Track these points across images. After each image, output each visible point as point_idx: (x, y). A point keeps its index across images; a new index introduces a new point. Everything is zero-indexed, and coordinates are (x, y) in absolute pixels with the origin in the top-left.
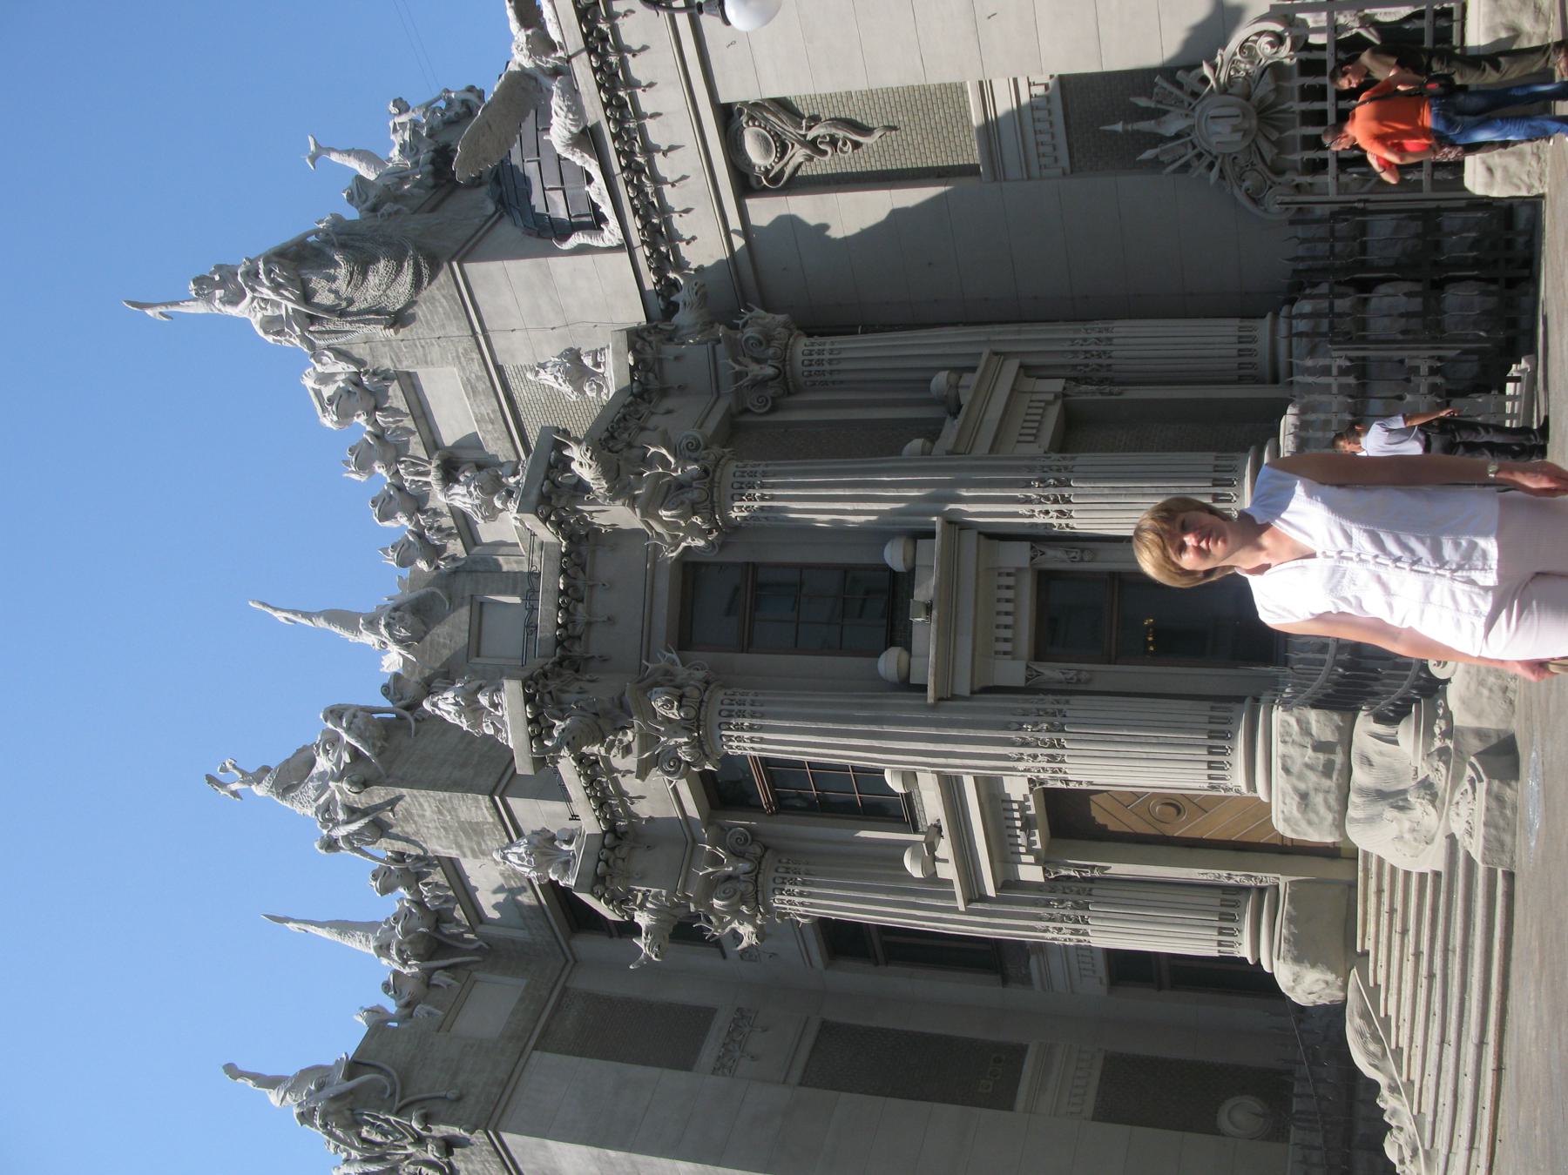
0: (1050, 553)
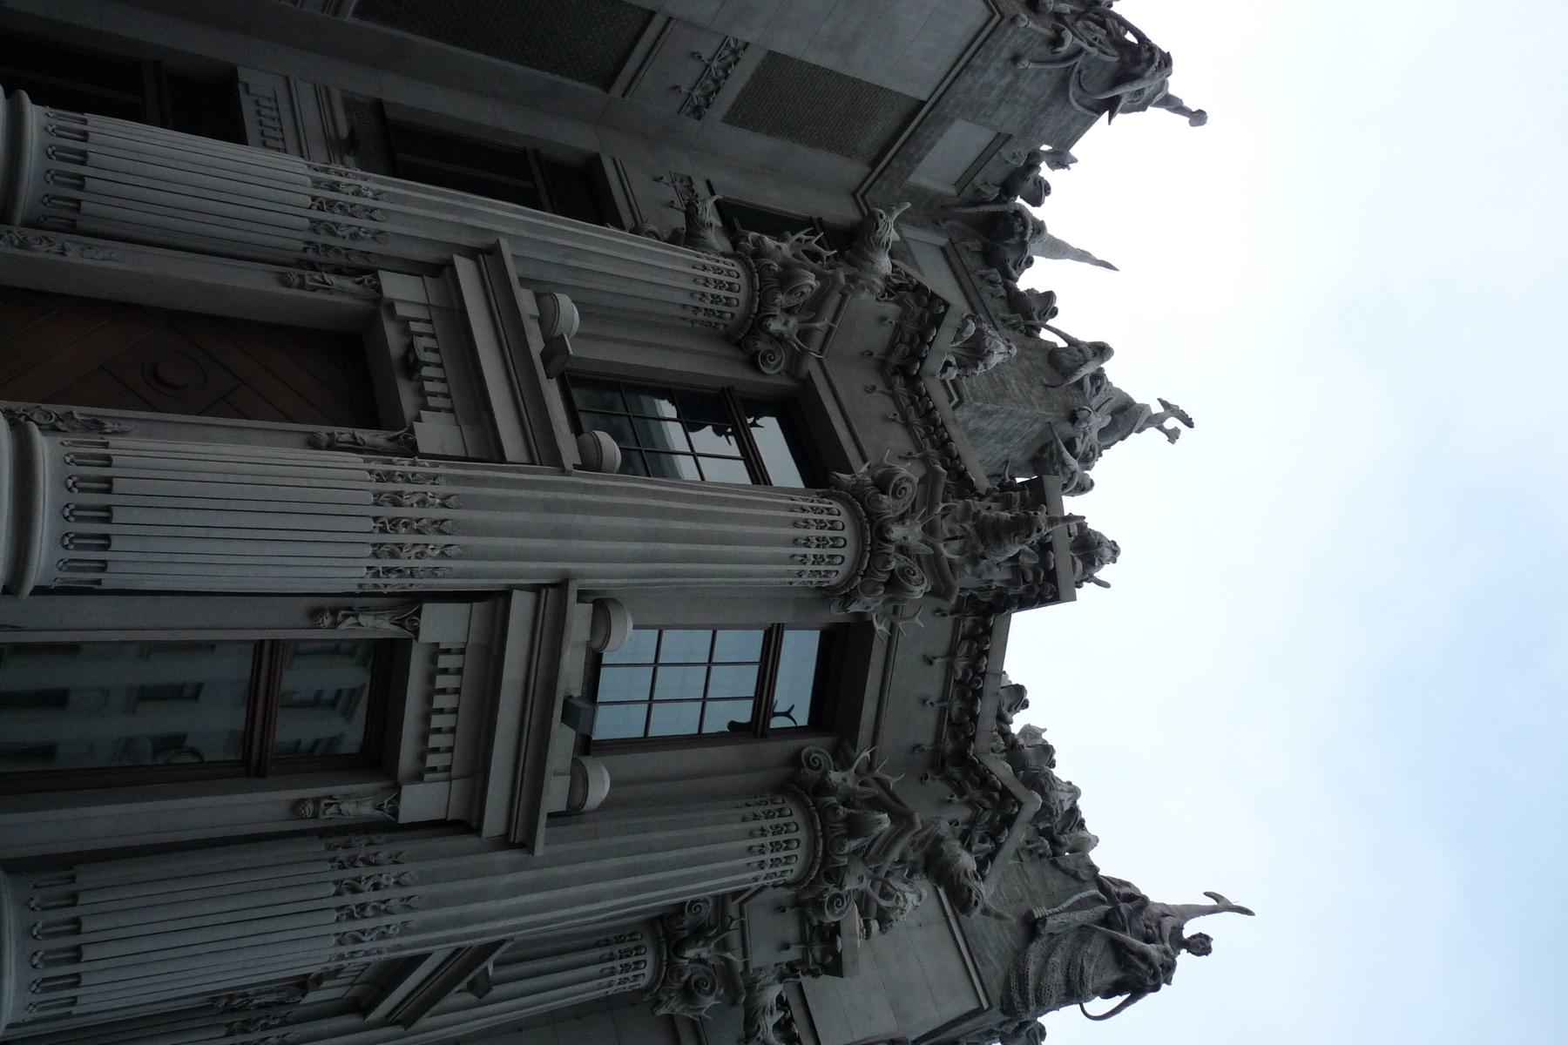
0: (367, 810)
